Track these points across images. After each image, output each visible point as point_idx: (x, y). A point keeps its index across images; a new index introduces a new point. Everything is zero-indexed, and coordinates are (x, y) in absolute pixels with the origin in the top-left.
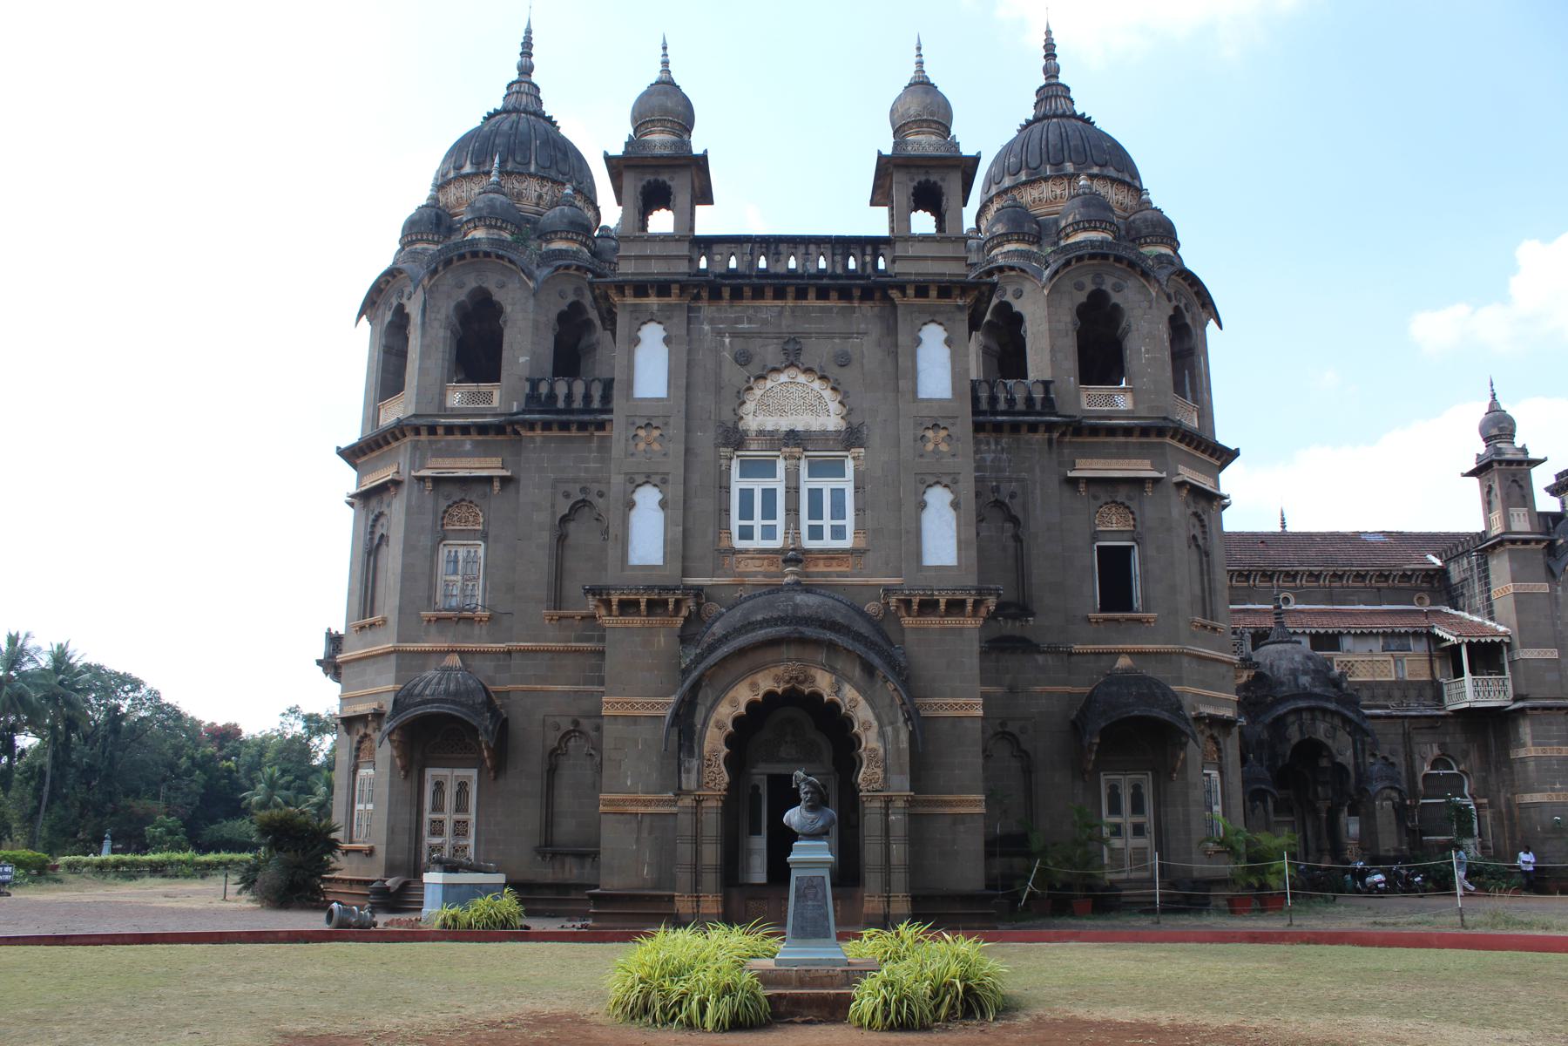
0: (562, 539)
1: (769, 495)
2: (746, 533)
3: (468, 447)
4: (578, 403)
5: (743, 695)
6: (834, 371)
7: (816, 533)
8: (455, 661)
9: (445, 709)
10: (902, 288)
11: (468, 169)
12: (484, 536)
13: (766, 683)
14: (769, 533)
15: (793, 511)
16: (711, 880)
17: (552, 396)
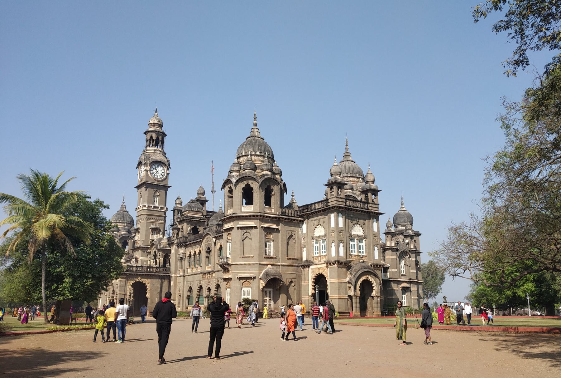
0: (288, 242)
1: (354, 245)
2: (352, 252)
4: (290, 215)
5: (361, 280)
6: (363, 225)
7: (360, 252)
8: (270, 266)
9: (277, 277)
10: (372, 212)
11: (258, 153)
12: (273, 241)
13: (364, 278)
14: (355, 252)
15: (358, 248)
16: (358, 309)
17: (285, 212)
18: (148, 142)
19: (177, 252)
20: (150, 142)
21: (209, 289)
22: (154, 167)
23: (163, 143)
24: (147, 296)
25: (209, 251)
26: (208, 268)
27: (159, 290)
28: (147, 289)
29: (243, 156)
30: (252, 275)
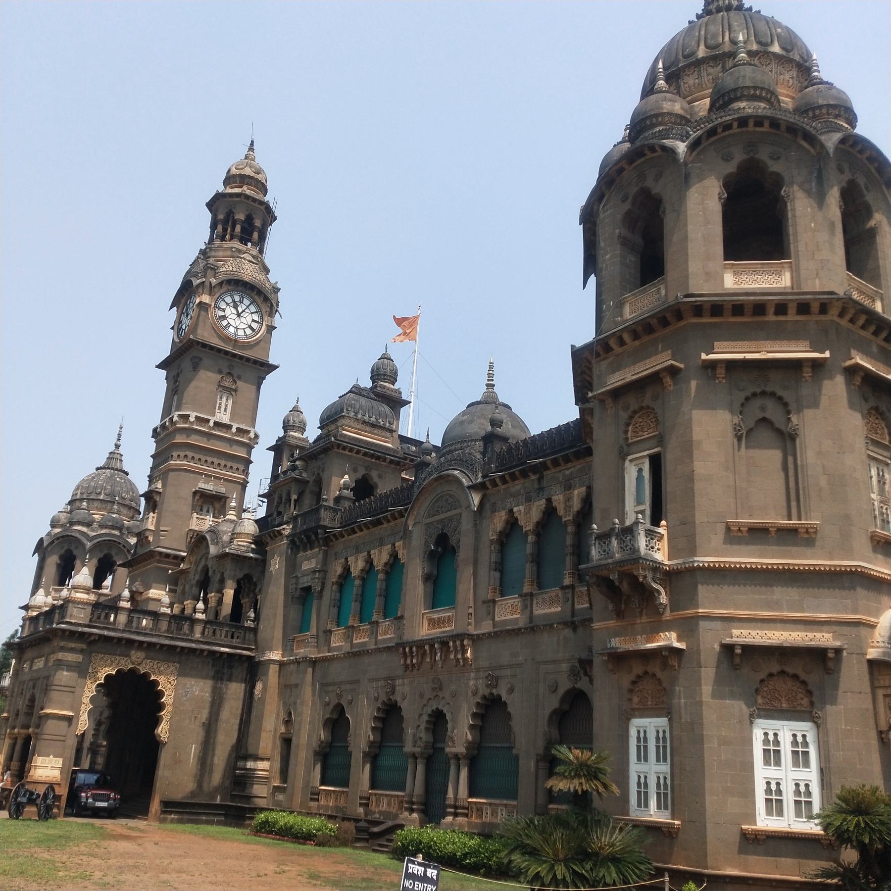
3: (875, 349)
18: (220, 228)
19: (292, 566)
20: (225, 230)
21: (438, 722)
22: (228, 299)
23: (262, 238)
24: (163, 730)
25: (442, 552)
26: (433, 623)
27: (204, 715)
28: (161, 707)
29: (699, 63)
30: (824, 639)
